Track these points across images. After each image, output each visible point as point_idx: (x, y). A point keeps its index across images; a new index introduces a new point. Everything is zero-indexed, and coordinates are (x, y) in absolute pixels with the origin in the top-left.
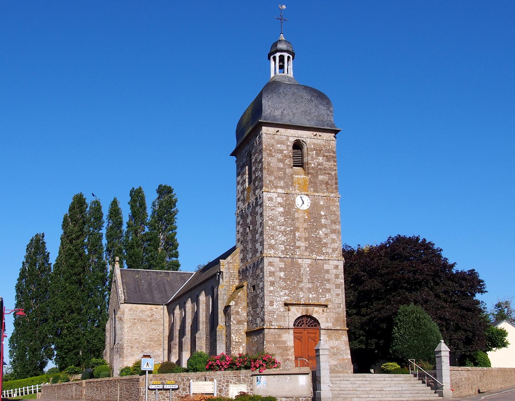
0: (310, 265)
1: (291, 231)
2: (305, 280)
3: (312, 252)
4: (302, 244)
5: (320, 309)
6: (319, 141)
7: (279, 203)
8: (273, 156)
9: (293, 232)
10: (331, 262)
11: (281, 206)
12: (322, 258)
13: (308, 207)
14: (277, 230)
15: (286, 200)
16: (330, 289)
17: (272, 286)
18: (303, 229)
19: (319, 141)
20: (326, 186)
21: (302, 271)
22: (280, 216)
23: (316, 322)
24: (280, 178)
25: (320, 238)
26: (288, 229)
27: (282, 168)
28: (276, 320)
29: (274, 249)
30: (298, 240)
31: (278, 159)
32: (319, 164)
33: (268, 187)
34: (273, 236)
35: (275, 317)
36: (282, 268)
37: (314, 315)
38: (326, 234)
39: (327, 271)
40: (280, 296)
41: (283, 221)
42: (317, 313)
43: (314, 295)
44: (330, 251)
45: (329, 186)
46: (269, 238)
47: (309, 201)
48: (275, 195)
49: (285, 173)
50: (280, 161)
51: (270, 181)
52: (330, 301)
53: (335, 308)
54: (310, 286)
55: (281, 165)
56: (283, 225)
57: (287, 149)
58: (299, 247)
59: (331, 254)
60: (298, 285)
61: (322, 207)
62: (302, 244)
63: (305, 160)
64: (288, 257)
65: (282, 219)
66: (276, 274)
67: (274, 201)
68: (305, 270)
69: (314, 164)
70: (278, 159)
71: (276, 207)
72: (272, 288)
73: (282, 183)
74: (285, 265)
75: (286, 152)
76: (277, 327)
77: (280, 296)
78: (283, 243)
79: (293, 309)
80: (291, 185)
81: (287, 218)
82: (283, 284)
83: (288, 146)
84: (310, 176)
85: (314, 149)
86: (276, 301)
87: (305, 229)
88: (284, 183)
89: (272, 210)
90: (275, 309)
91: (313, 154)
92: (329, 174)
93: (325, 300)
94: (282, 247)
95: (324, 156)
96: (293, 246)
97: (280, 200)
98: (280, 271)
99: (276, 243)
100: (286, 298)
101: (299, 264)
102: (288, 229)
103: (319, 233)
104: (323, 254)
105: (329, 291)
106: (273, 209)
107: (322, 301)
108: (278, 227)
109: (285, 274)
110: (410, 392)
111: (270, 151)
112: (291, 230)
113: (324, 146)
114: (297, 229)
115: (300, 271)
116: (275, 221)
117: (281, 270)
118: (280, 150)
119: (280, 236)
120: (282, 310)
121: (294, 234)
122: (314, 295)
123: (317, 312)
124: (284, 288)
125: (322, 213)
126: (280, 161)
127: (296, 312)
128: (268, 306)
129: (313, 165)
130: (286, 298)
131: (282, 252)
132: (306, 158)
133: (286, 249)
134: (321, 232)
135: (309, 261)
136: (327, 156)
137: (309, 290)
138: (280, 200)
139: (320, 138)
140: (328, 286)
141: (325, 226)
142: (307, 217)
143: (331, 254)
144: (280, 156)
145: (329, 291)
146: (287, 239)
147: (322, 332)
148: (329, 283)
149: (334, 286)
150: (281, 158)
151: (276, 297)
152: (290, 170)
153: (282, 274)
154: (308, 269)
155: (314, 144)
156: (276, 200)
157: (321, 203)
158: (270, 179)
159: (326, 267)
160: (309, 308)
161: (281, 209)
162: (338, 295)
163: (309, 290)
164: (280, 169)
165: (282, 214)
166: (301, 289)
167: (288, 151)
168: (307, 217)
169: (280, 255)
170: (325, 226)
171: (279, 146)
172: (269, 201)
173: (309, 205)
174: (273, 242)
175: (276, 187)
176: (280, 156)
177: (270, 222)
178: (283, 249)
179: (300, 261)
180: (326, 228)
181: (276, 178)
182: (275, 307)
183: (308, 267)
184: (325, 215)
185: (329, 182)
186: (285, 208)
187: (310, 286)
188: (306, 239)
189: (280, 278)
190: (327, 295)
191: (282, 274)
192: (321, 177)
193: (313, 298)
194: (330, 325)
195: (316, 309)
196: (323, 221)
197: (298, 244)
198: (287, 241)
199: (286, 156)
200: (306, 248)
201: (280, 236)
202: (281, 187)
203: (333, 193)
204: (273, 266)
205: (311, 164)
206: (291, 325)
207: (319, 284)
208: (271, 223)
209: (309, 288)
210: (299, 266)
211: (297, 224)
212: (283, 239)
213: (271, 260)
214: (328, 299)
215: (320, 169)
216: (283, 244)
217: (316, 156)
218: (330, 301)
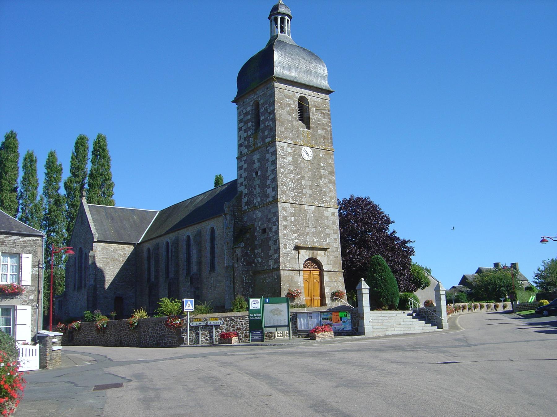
0: (313, 211)
2: (311, 225)
3: (315, 199)
4: (307, 191)
5: (322, 253)
8: (283, 109)
14: (287, 177)
23: (319, 265)
24: (289, 130)
34: (284, 182)
36: (292, 213)
37: (319, 258)
38: (325, 184)
39: (327, 218)
40: (292, 240)
42: (320, 256)
44: (328, 199)
45: (326, 141)
47: (312, 153)
48: (286, 145)
49: (292, 125)
53: (333, 252)
56: (292, 173)
58: (305, 195)
61: (321, 159)
65: (291, 167)
66: (288, 219)
72: (285, 232)
73: (290, 135)
74: (295, 211)
77: (292, 240)
79: (302, 252)
82: (294, 228)
87: (309, 178)
89: (284, 158)
95: (321, 113)
99: (287, 190)
100: (296, 241)
104: (323, 202)
105: (328, 235)
107: (324, 245)
111: (281, 103)
113: (322, 104)
114: (303, 178)
115: (306, 216)
117: (292, 215)
124: (294, 232)
125: (322, 165)
127: (305, 255)
130: (296, 241)
133: (295, 195)
136: (324, 113)
138: (289, 149)
140: (328, 231)
144: (288, 109)
145: (328, 235)
146: (295, 187)
152: (297, 123)
153: (293, 219)
158: (282, 130)
159: (326, 213)
162: (335, 240)
164: (289, 121)
165: (291, 162)
169: (291, 201)
171: (287, 100)
175: (286, 138)
176: (288, 109)
181: (286, 129)
182: (288, 249)
188: (310, 188)
189: (291, 222)
191: (293, 219)
192: (320, 132)
193: (317, 242)
194: (330, 268)
202: (290, 138)
204: (285, 211)
213: (284, 205)
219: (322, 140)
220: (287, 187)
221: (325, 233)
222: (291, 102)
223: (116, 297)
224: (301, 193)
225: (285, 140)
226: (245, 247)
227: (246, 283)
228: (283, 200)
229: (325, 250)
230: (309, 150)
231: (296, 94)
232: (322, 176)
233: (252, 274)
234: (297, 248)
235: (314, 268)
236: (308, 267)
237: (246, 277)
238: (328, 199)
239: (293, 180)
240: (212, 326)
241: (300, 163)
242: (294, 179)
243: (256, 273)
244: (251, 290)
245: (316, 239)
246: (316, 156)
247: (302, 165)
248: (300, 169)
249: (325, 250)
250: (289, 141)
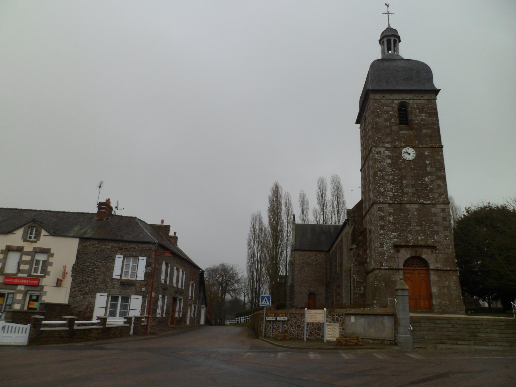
0: (417, 209)
1: (399, 179)
3: (419, 197)
5: (429, 251)
6: (421, 101)
7: (387, 156)
8: (381, 117)
9: (401, 180)
10: (438, 206)
11: (389, 158)
12: (429, 202)
13: (413, 158)
14: (385, 179)
19: (421, 101)
21: (410, 215)
23: (425, 263)
24: (387, 135)
25: (426, 184)
28: (387, 261)
30: (405, 187)
31: (385, 119)
32: (422, 120)
34: (381, 184)
35: (386, 258)
36: (391, 212)
37: (424, 256)
38: (432, 181)
39: (435, 215)
40: (390, 239)
44: (436, 196)
47: (414, 152)
48: (383, 149)
49: (391, 130)
50: (386, 120)
51: (378, 138)
54: (419, 228)
55: (388, 124)
56: (391, 175)
58: (407, 194)
59: (438, 198)
62: (410, 190)
63: (410, 118)
65: (389, 169)
67: (382, 154)
69: (418, 120)
70: (385, 119)
71: (384, 159)
72: (382, 232)
74: (394, 210)
76: (387, 268)
77: (390, 239)
78: (391, 190)
80: (397, 140)
82: (392, 227)
83: (393, 108)
84: (414, 131)
85: (418, 108)
86: (386, 244)
87: (412, 177)
88: (391, 138)
89: (380, 162)
92: (431, 128)
93: (434, 242)
95: (426, 113)
96: (400, 193)
97: (387, 153)
98: (390, 216)
99: (385, 191)
100: (395, 240)
101: (407, 209)
103: (425, 180)
104: (430, 199)
105: (437, 233)
106: (382, 161)
107: (431, 242)
109: (394, 219)
111: (378, 112)
113: (426, 104)
114: (404, 177)
115: (408, 215)
117: (390, 214)
118: (386, 111)
120: (392, 251)
121: (402, 183)
123: (426, 253)
124: (393, 231)
125: (428, 162)
126: (386, 120)
127: (405, 254)
129: (416, 122)
130: (395, 240)
131: (391, 198)
133: (394, 195)
134: (427, 179)
135: (416, 206)
136: (429, 113)
138: (387, 153)
139: (422, 98)
140: (436, 228)
141: (430, 173)
143: (438, 198)
144: (386, 116)
145: (437, 233)
146: (395, 187)
147: (432, 273)
152: (396, 127)
154: (416, 213)
155: (417, 104)
157: (426, 153)
158: (378, 136)
159: (433, 210)
160: (418, 249)
161: (389, 161)
162: (446, 236)
163: (418, 233)
165: (389, 165)
166: (410, 232)
167: (393, 111)
169: (389, 201)
170: (430, 173)
171: (385, 108)
173: (414, 155)
174: (382, 190)
175: (384, 143)
176: (386, 116)
179: (408, 206)
181: (383, 135)
182: (385, 249)
183: (416, 211)
186: (392, 160)
187: (419, 228)
188: (413, 186)
189: (390, 222)
191: (391, 219)
192: (424, 131)
193: (422, 240)
194: (439, 266)
195: (425, 250)
196: (428, 169)
197: (406, 190)
199: (391, 116)
200: (413, 193)
202: (388, 142)
204: (382, 211)
205: (415, 120)
206: (401, 266)
209: (417, 231)
210: (408, 210)
212: (391, 187)
213: (381, 206)
215: (424, 124)
216: (392, 192)
218: (439, 242)
219: (428, 139)
220: (385, 188)
221: (433, 231)
222: (389, 109)
223: (310, 293)
224: (402, 192)
225: (381, 145)
226: (356, 248)
227: (357, 282)
228: (380, 201)
229: (433, 247)
230: (411, 151)
231: (396, 102)
232: (427, 174)
233: (364, 274)
234: (397, 247)
235: (419, 267)
236: (411, 266)
237: (357, 277)
238: (436, 196)
239: (392, 181)
241: (401, 164)
242: (393, 180)
243: (367, 273)
244: (362, 288)
245: (421, 236)
246: (419, 155)
247: (403, 165)
248: (400, 170)
249: (433, 247)
250: (387, 145)
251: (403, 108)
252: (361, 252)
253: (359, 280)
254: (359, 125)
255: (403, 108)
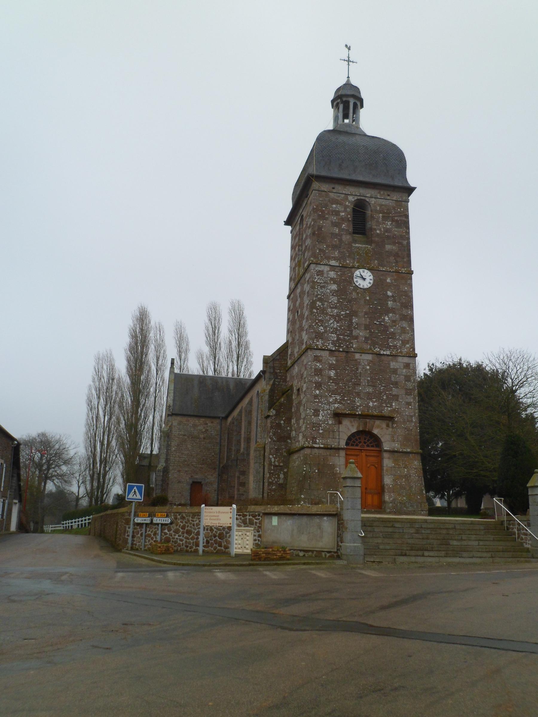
0: (370, 362)
1: (346, 315)
2: (364, 382)
3: (374, 344)
4: (362, 333)
6: (387, 202)
7: (332, 279)
8: (326, 219)
9: (349, 317)
10: (400, 359)
11: (334, 283)
12: (388, 353)
13: (369, 285)
14: (327, 314)
15: (341, 274)
16: (398, 396)
17: (318, 389)
18: (363, 314)
19: (387, 202)
20: (395, 259)
21: (360, 370)
22: (333, 295)
23: (376, 441)
24: (335, 247)
25: (385, 326)
26: (342, 313)
27: (336, 235)
28: (322, 436)
29: (322, 339)
30: (355, 328)
31: (332, 222)
32: (387, 230)
33: (318, 258)
34: (320, 321)
35: (321, 431)
36: (332, 364)
37: (375, 431)
38: (394, 321)
39: (395, 371)
40: (329, 403)
41: (336, 302)
42: (379, 429)
43: (375, 404)
44: (399, 344)
45: (398, 259)
46: (317, 323)
47: (372, 277)
48: (327, 268)
49: (341, 240)
50: (335, 224)
51: (320, 250)
52: (397, 412)
53: (404, 422)
54: (371, 390)
55: (337, 231)
56: (336, 308)
57: (345, 211)
58: (356, 338)
59: (401, 348)
60: (354, 388)
61: (389, 286)
62: (362, 333)
63: (368, 225)
64: (341, 350)
65: (334, 299)
66: (324, 373)
67: (325, 275)
68: (363, 368)
69: (380, 230)
70: (332, 222)
71: (327, 283)
72: (318, 392)
73: (336, 254)
74: (337, 361)
75: (343, 214)
76: (322, 446)
77: (329, 403)
78: (335, 331)
79: (346, 422)
80: (349, 256)
81: (342, 299)
82: (333, 386)
83: (346, 207)
84: (373, 245)
85: (380, 212)
86: (323, 410)
87: (366, 313)
88: (339, 252)
89: (322, 287)
90: (321, 421)
91: (379, 217)
92: (398, 243)
93: (391, 411)
94: (334, 337)
95: (393, 221)
96: (348, 336)
97: (332, 274)
98: (330, 369)
99: (326, 331)
100: (336, 405)
101: (356, 360)
102: (342, 313)
103: (384, 319)
104: (389, 347)
105: (396, 398)
106: (324, 287)
107: (386, 411)
108: (329, 310)
109: (336, 374)
110: (419, 565)
111: (323, 212)
112: (346, 314)
113: (394, 208)
114: (354, 313)
115: (357, 369)
116: (325, 301)
117: (331, 367)
118: (335, 211)
119: (332, 321)
120: (330, 422)
121: (351, 320)
122: (375, 404)
123: (378, 427)
124: (334, 392)
125: (389, 293)
126: (335, 224)
127: (349, 428)
128: (311, 416)
129: (378, 232)
130: (336, 405)
131: (334, 343)
132: (370, 223)
133: (339, 339)
134: (387, 318)
135: (369, 357)
136: (397, 221)
137: (369, 396)
138: (332, 274)
139: (388, 198)
140: (395, 391)
141: (392, 310)
142: (368, 298)
143: (401, 348)
145: (396, 398)
146: (340, 326)
147: (385, 455)
148: (397, 388)
149: (403, 392)
150: (337, 221)
151: (322, 404)
152: (348, 237)
153: (332, 373)
154: (368, 367)
155: (381, 205)
156: (328, 274)
157: (388, 280)
158: (321, 247)
159: (393, 365)
160: (368, 420)
161: (334, 287)
162: (409, 404)
163: (369, 396)
164: (333, 235)
165: (334, 293)
166: (358, 395)
167: (345, 212)
168: (368, 298)
169: (331, 347)
170: (392, 310)
171: (334, 206)
172: (318, 275)
173: (372, 282)
174: (321, 329)
175: (329, 258)
177: (318, 303)
178: (335, 339)
179: (357, 356)
180: (394, 313)
181: (328, 246)
183: (369, 365)
184: (393, 296)
185: (400, 253)
186: (339, 286)
187: (371, 390)
188: (367, 327)
189: (330, 378)
190: (394, 404)
192: (388, 247)
193: (374, 407)
194: (396, 446)
195: (378, 422)
196: (390, 303)
197: (355, 333)
198: (341, 328)
199: (343, 219)
200: (366, 338)
201: (332, 321)
202: (335, 259)
203: (404, 267)
204: (320, 361)
205: (375, 230)
206: (343, 444)
207: (382, 388)
208: (320, 304)
209: (369, 393)
210: (357, 363)
211: (355, 308)
212: (335, 326)
213: (318, 353)
214: (394, 410)
215: (388, 237)
216: (336, 333)
217: (383, 220)
218: (397, 412)
219: (392, 259)
220: (325, 327)
221: (391, 394)
222: (340, 208)
223: (193, 482)
224: (350, 335)
225: (325, 262)
226: (276, 415)
227: (275, 466)
228: (317, 345)
229: (389, 419)
230: (367, 274)
231: (351, 198)
232: (388, 311)
233: (285, 454)
234: (338, 416)
235: (368, 446)
236: (357, 445)
237: (275, 458)
238: (399, 344)
239: (337, 318)
240: (158, 524)
241: (351, 293)
242: (338, 315)
243: (291, 453)
244: (282, 476)
245: (374, 402)
246: (378, 283)
247: (354, 295)
248: (350, 301)
249: (389, 419)
250: (333, 263)
251: (360, 210)
252: (282, 422)
253: (277, 464)
254: (289, 228)
255: (360, 210)
